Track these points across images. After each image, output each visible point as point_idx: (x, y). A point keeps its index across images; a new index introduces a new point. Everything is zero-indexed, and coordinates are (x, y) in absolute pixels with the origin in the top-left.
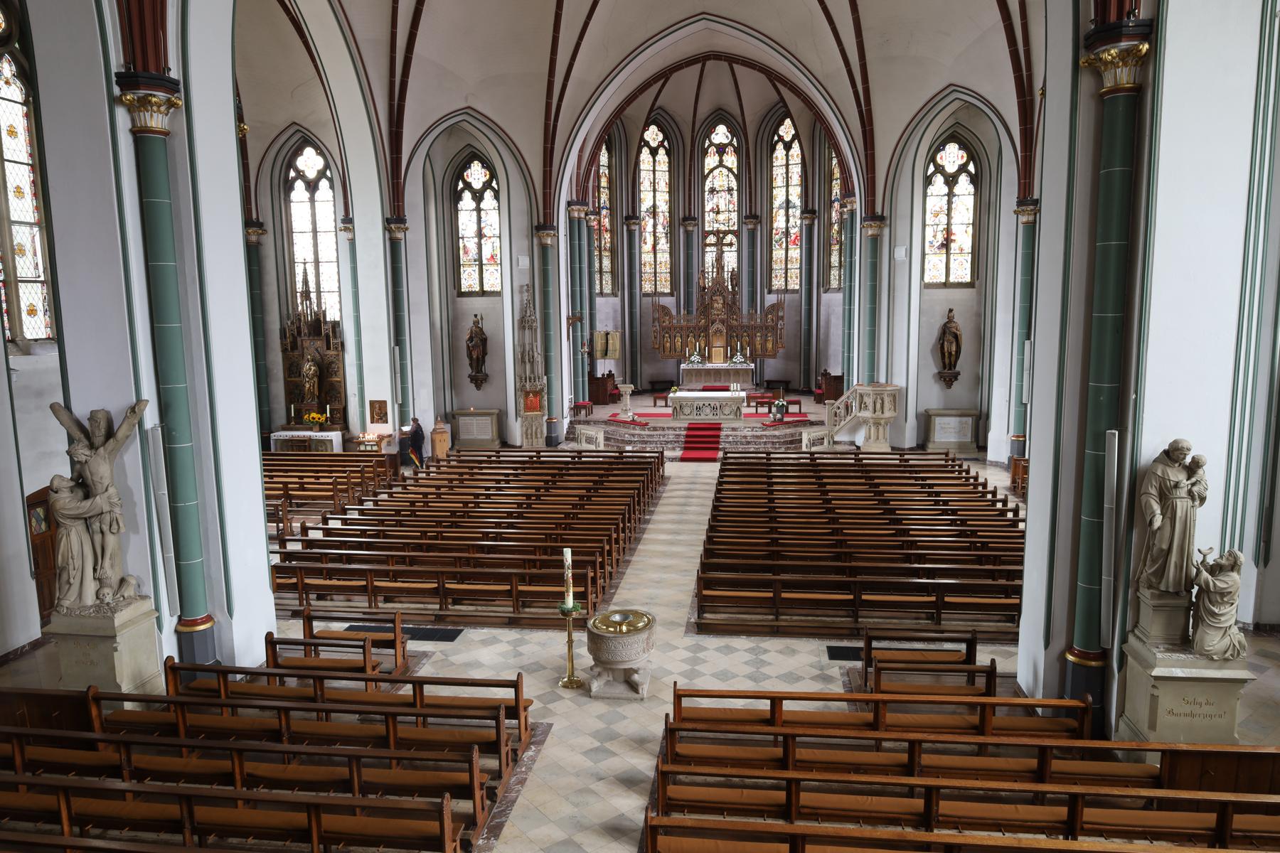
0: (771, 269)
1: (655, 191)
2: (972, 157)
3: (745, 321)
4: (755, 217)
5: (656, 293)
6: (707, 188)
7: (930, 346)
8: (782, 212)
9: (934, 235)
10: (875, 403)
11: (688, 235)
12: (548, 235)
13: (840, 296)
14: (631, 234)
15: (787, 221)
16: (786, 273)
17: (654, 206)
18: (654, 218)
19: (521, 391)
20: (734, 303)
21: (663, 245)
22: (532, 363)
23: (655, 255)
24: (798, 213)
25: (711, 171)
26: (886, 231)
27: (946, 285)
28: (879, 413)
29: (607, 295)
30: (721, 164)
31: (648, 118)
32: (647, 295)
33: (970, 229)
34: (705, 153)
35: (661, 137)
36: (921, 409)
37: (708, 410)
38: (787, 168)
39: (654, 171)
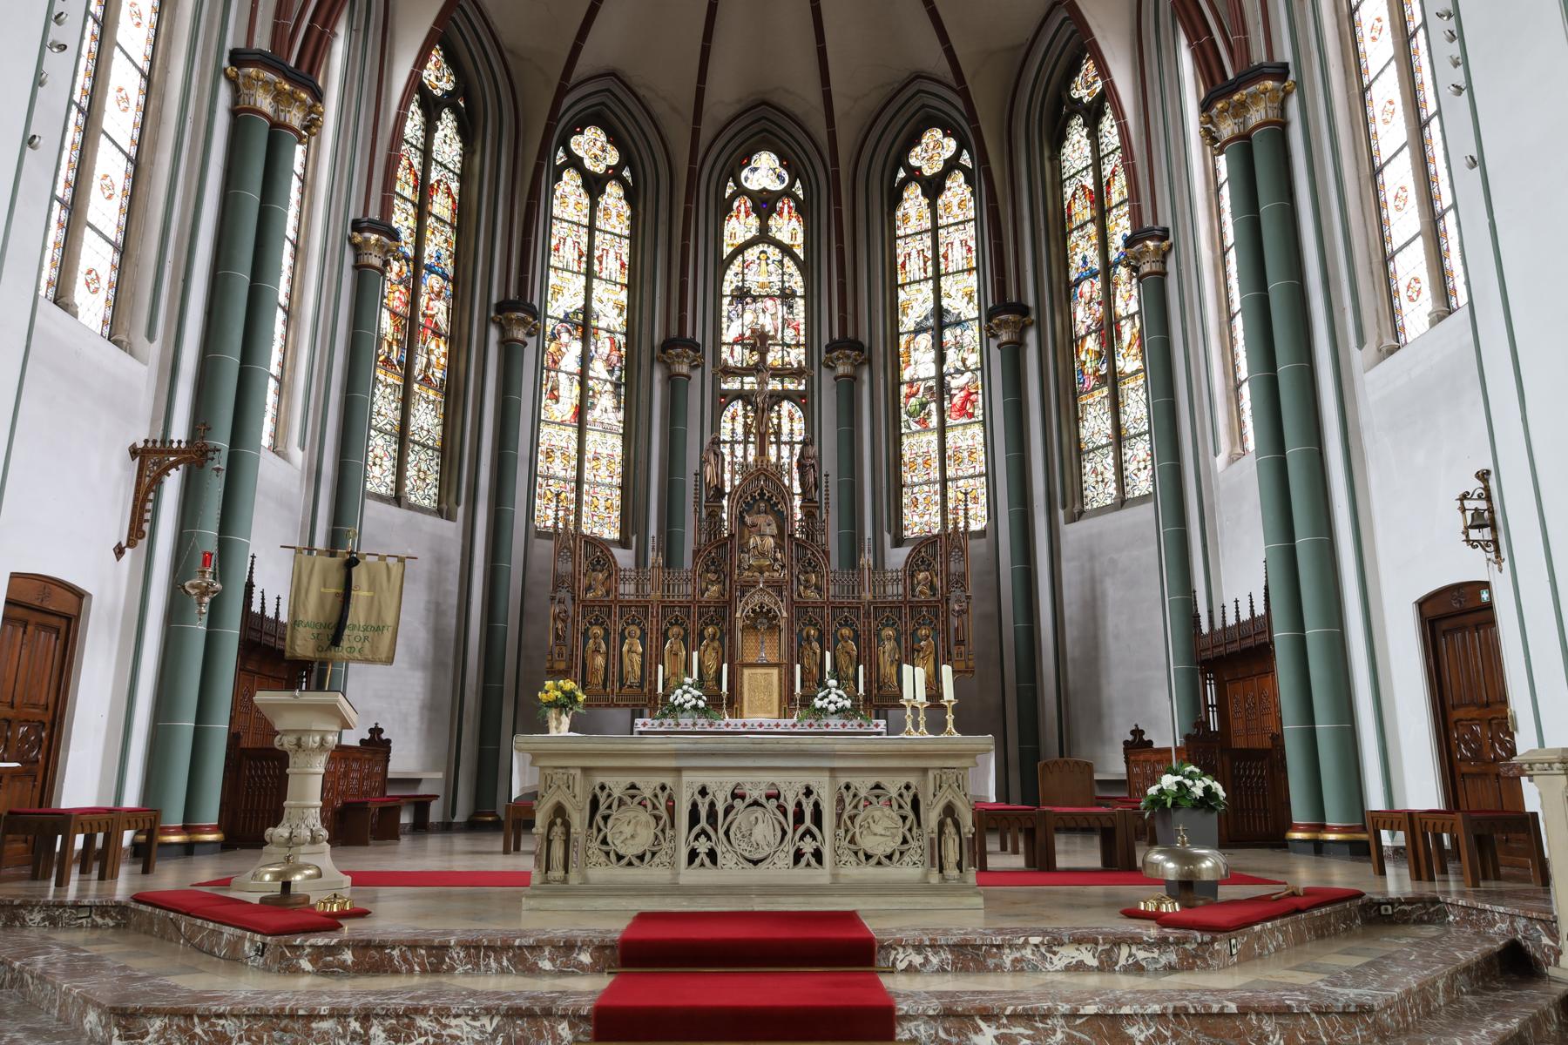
0: (898, 486)
4: (856, 345)
6: (727, 289)
8: (925, 340)
11: (675, 384)
14: (510, 351)
15: (941, 359)
17: (587, 309)
18: (585, 339)
21: (606, 410)
24: (972, 335)
25: (740, 250)
30: (764, 236)
34: (725, 209)
37: (762, 829)
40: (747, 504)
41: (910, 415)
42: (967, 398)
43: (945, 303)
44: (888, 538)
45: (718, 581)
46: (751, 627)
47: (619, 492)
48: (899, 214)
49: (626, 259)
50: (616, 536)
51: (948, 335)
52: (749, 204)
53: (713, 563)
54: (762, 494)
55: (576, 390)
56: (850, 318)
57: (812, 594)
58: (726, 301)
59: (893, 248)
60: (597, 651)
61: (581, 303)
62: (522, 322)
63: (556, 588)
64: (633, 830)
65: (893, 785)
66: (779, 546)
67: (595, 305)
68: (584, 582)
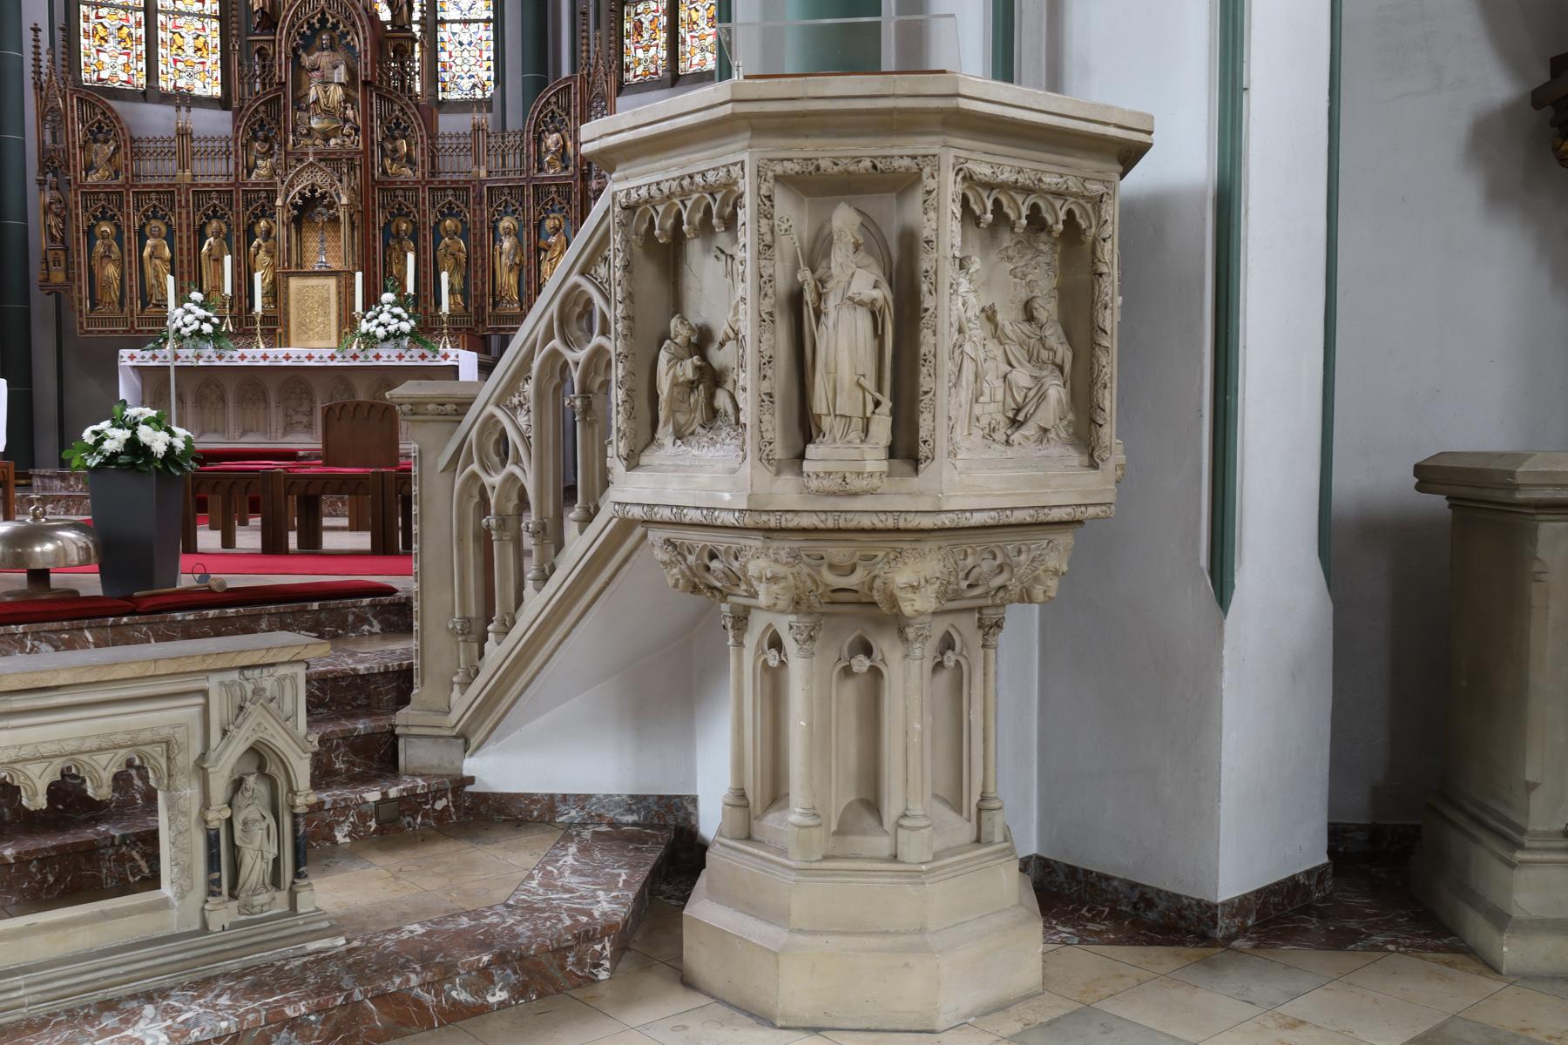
10: (798, 311)
28: (852, 454)
40: (302, 36)
45: (268, 154)
47: (216, 24)
50: (217, 91)
53: (262, 126)
54: (323, 21)
60: (106, 256)
66: (348, 99)
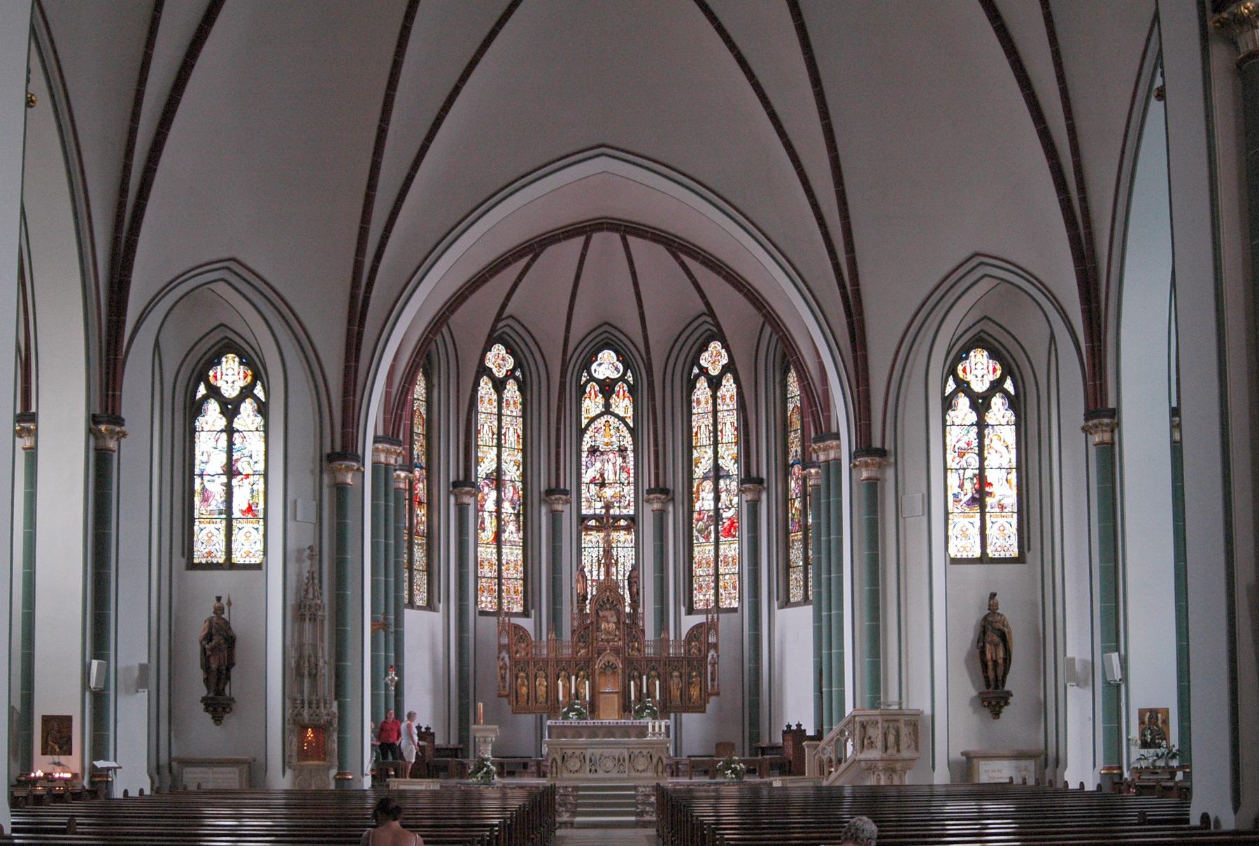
1: (499, 446)
2: (1008, 371)
3: (649, 651)
4: (665, 491)
5: (498, 613)
6: (585, 447)
7: (964, 654)
8: (708, 485)
9: (959, 484)
11: (555, 517)
12: (349, 469)
13: (808, 610)
14: (462, 509)
15: (717, 499)
16: (717, 581)
17: (499, 469)
19: (295, 724)
20: (635, 623)
21: (512, 533)
22: (313, 677)
23: (498, 550)
24: (734, 485)
25: (593, 420)
26: (890, 473)
27: (984, 559)
29: (420, 608)
30: (607, 410)
31: (490, 336)
32: (483, 613)
33: (1013, 476)
34: (581, 391)
35: (510, 363)
36: (956, 755)
37: (610, 764)
38: (715, 423)
39: (500, 415)
41: (700, 532)
42: (731, 525)
43: (720, 461)
44: (683, 609)
46: (603, 671)
48: (694, 398)
49: (520, 433)
51: (722, 482)
52: (597, 388)
55: (494, 523)
56: (661, 472)
57: (636, 653)
58: (584, 455)
59: (690, 421)
60: (523, 685)
61: (494, 466)
62: (468, 493)
63: (500, 652)
64: (574, 764)
65: (645, 752)
66: (618, 628)
67: (504, 466)
68: (514, 649)
